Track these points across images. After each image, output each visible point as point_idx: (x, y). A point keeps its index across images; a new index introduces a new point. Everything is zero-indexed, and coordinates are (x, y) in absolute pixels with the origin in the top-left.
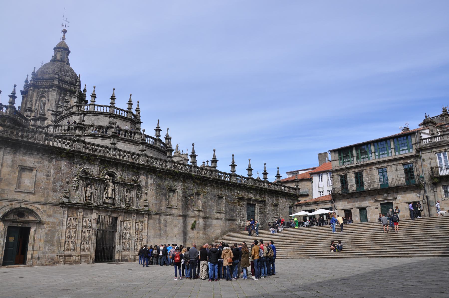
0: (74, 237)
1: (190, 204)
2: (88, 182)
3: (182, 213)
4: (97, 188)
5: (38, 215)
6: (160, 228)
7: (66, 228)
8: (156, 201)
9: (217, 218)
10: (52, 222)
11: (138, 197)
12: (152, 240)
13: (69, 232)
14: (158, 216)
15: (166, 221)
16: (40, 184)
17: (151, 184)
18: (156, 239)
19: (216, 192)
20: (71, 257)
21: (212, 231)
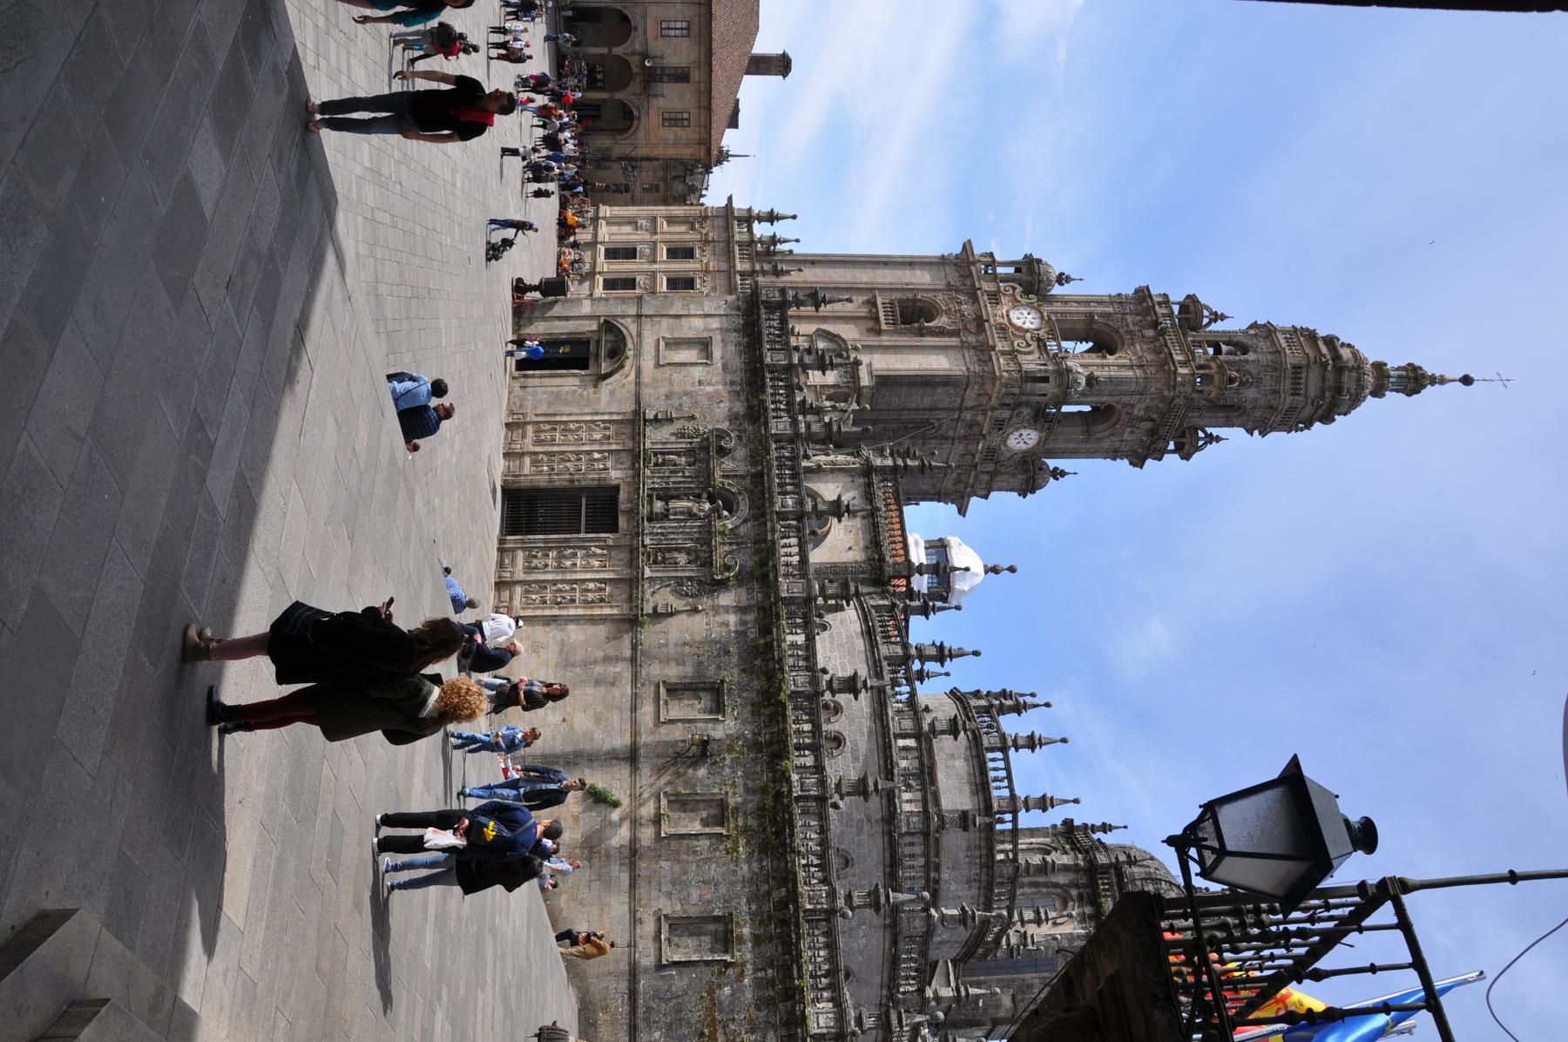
1: (678, 775)
3: (646, 745)
4: (687, 474)
6: (591, 663)
7: (586, 422)
8: (676, 645)
9: (635, 921)
10: (599, 399)
11: (680, 581)
12: (554, 638)
13: (580, 428)
14: (627, 653)
15: (613, 684)
17: (726, 624)
18: (556, 648)
19: (745, 908)
21: (584, 893)
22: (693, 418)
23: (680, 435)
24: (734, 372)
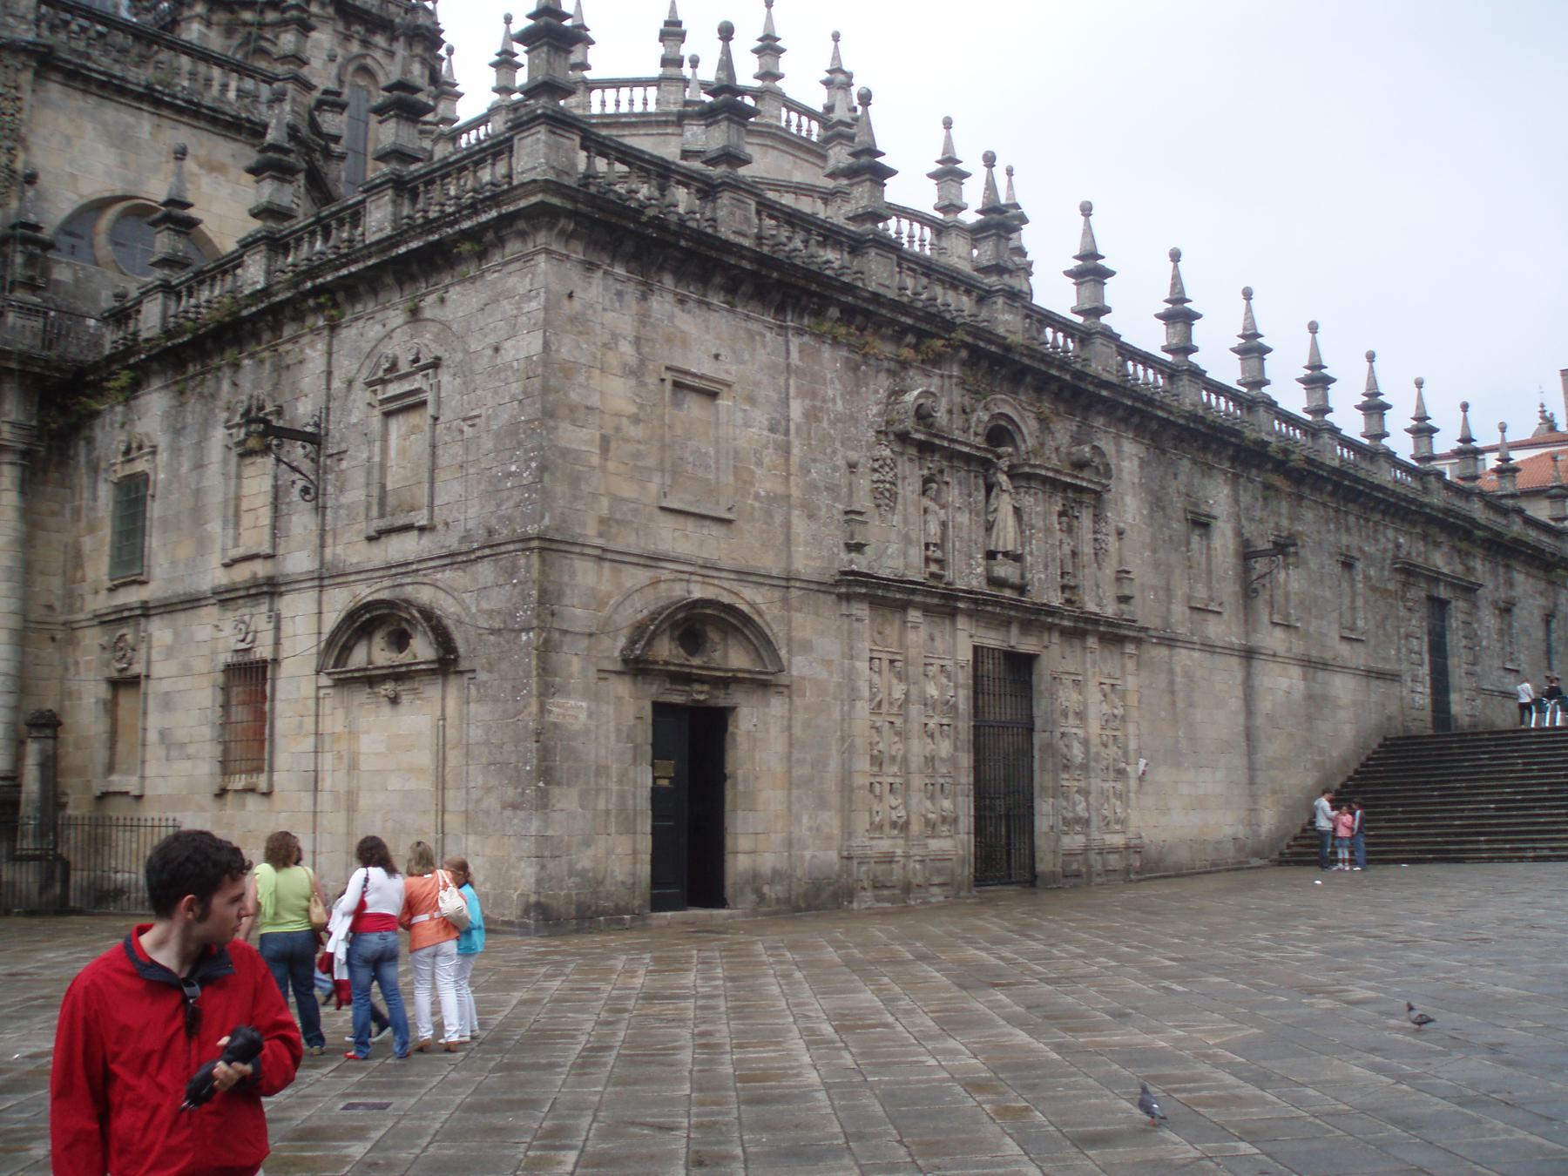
0: (899, 759)
2: (929, 468)
5: (768, 642)
16: (752, 473)
20: (890, 862)
22: (852, 466)
23: (886, 496)
24: (751, 336)
